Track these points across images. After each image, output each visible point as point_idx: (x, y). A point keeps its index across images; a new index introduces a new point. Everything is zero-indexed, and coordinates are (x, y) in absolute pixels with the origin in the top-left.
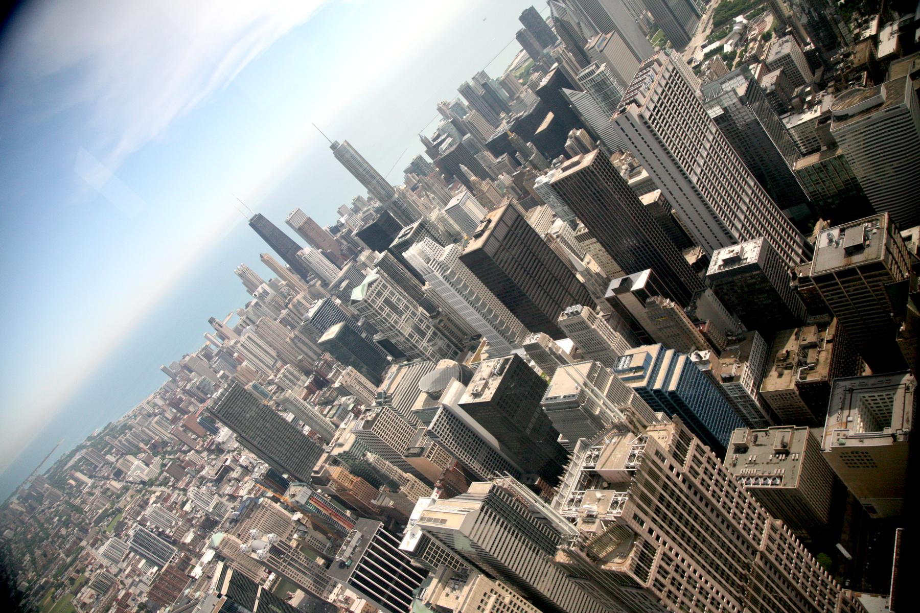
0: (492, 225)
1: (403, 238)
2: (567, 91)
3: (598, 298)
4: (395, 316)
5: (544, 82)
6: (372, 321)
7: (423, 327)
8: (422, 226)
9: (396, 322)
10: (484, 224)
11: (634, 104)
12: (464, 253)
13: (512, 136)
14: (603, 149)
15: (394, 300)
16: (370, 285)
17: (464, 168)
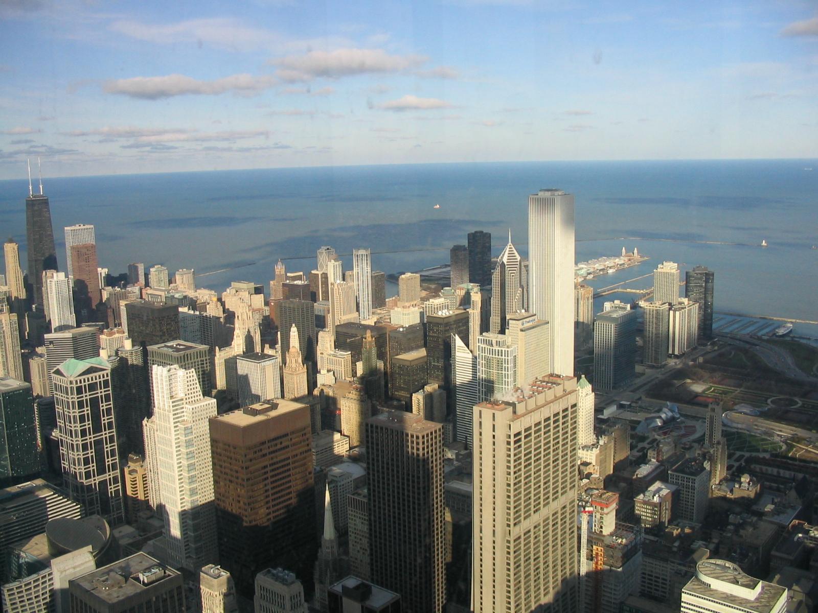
0: (273, 414)
1: (170, 350)
2: (458, 342)
3: (321, 582)
4: (88, 424)
5: (443, 313)
6: (59, 409)
7: (109, 461)
9: (84, 433)
10: (267, 406)
11: (511, 409)
12: (220, 418)
13: (369, 339)
14: (450, 427)
15: (103, 406)
17: (294, 332)
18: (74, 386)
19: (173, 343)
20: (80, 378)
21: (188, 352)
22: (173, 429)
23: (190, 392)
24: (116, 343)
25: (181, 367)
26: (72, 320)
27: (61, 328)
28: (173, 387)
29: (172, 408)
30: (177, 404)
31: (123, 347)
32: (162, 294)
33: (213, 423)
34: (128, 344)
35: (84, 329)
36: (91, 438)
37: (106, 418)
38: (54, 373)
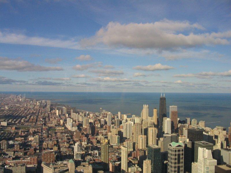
4: (177, 161)
6: (169, 155)
8: (211, 146)
15: (181, 156)
16: (179, 146)
18: (174, 149)
19: (203, 142)
20: (176, 148)
21: (207, 145)
22: (203, 167)
23: (209, 156)
24: (184, 140)
25: (207, 149)
26: (170, 132)
27: (167, 134)
28: (203, 154)
29: (203, 161)
30: (205, 159)
31: (186, 141)
32: (196, 127)
33: (216, 167)
34: (188, 140)
35: (174, 134)
36: (177, 165)
37: (181, 160)
38: (169, 145)
